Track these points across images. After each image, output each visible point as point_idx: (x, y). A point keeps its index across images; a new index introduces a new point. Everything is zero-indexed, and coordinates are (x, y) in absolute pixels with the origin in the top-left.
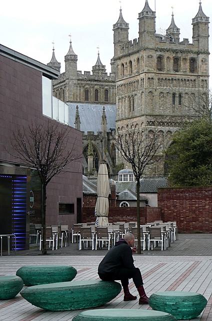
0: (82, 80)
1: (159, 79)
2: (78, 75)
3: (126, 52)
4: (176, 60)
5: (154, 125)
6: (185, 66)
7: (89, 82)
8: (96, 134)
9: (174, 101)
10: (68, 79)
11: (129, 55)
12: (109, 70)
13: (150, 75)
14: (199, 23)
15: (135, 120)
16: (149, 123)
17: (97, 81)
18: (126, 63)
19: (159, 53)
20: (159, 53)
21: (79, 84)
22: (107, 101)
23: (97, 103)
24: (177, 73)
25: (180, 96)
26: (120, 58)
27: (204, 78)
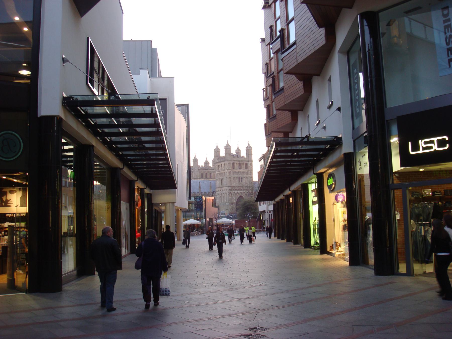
0: (200, 169)
1: (233, 172)
2: (198, 167)
3: (219, 161)
4: (240, 164)
5: (231, 190)
6: (243, 167)
7: (203, 170)
8: (207, 193)
9: (239, 180)
10: (194, 169)
11: (221, 162)
12: (211, 165)
13: (229, 171)
15: (224, 188)
16: (229, 190)
17: (206, 169)
18: (220, 165)
19: (233, 162)
21: (199, 171)
22: (211, 177)
23: (207, 179)
24: (240, 169)
25: (242, 178)
26: (217, 163)
27: (251, 171)
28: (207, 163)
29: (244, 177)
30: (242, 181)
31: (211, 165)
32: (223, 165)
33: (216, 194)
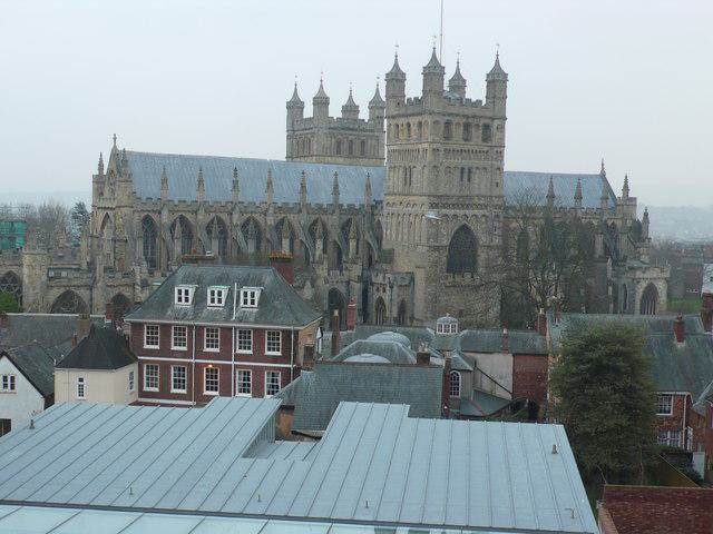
3: (403, 111)
4: (467, 126)
6: (477, 134)
9: (462, 178)
11: (408, 116)
12: (364, 114)
14: (497, 81)
15: (412, 198)
17: (352, 130)
19: (446, 118)
20: (446, 118)
25: (470, 172)
26: (393, 117)
28: (351, 108)
29: (477, 168)
30: (469, 180)
31: (364, 114)
32: (414, 128)
33: (385, 211)
